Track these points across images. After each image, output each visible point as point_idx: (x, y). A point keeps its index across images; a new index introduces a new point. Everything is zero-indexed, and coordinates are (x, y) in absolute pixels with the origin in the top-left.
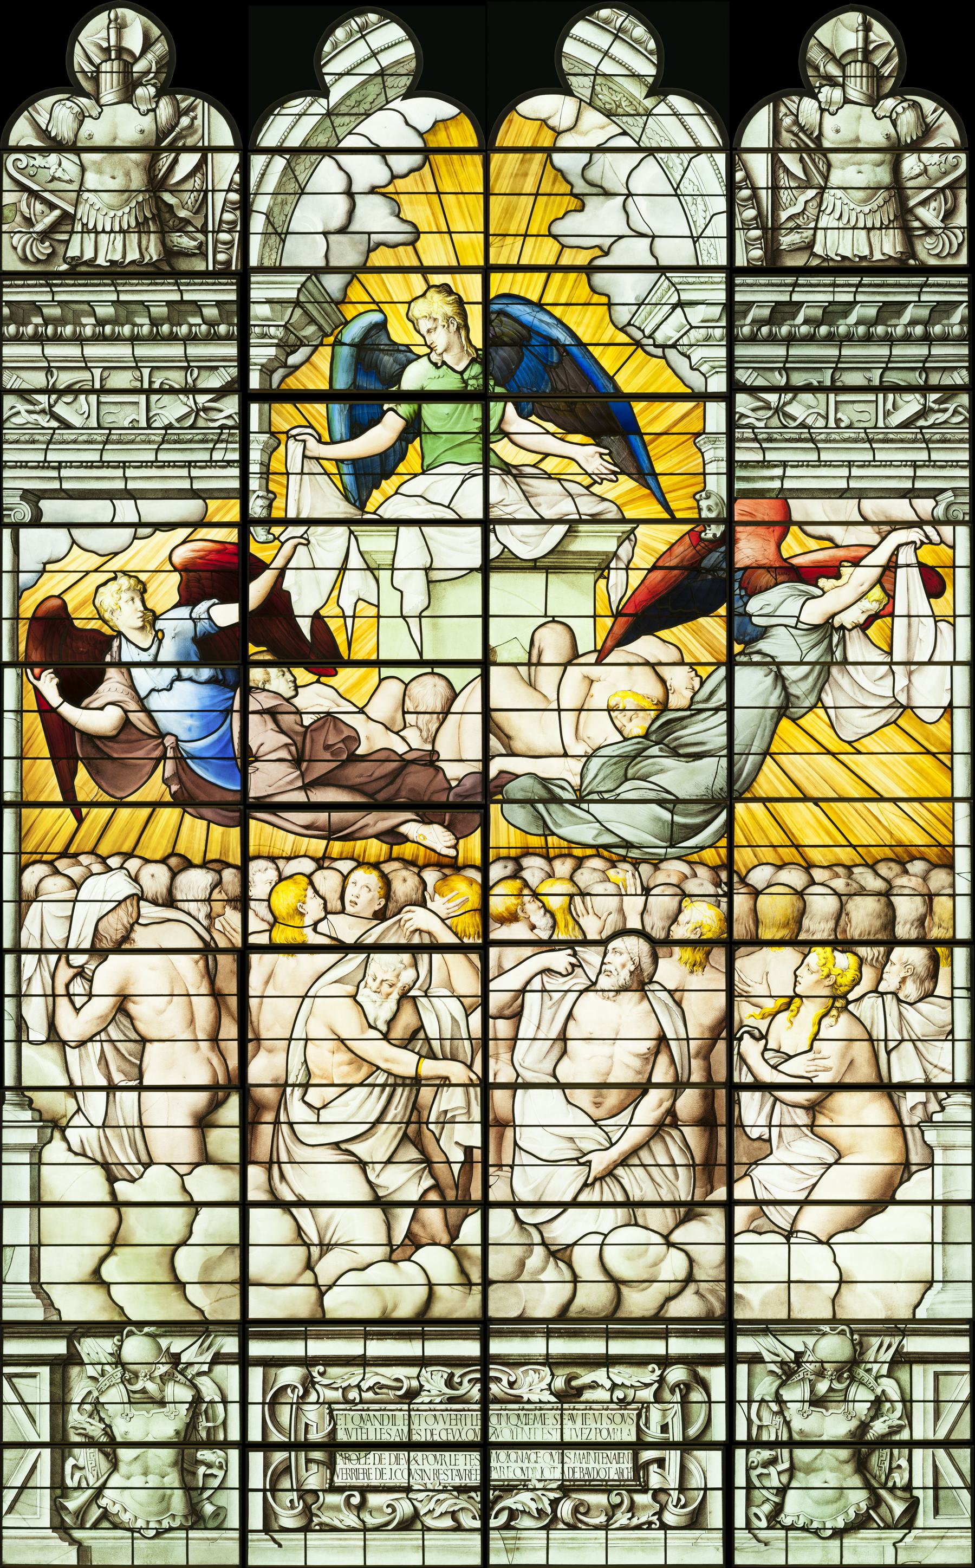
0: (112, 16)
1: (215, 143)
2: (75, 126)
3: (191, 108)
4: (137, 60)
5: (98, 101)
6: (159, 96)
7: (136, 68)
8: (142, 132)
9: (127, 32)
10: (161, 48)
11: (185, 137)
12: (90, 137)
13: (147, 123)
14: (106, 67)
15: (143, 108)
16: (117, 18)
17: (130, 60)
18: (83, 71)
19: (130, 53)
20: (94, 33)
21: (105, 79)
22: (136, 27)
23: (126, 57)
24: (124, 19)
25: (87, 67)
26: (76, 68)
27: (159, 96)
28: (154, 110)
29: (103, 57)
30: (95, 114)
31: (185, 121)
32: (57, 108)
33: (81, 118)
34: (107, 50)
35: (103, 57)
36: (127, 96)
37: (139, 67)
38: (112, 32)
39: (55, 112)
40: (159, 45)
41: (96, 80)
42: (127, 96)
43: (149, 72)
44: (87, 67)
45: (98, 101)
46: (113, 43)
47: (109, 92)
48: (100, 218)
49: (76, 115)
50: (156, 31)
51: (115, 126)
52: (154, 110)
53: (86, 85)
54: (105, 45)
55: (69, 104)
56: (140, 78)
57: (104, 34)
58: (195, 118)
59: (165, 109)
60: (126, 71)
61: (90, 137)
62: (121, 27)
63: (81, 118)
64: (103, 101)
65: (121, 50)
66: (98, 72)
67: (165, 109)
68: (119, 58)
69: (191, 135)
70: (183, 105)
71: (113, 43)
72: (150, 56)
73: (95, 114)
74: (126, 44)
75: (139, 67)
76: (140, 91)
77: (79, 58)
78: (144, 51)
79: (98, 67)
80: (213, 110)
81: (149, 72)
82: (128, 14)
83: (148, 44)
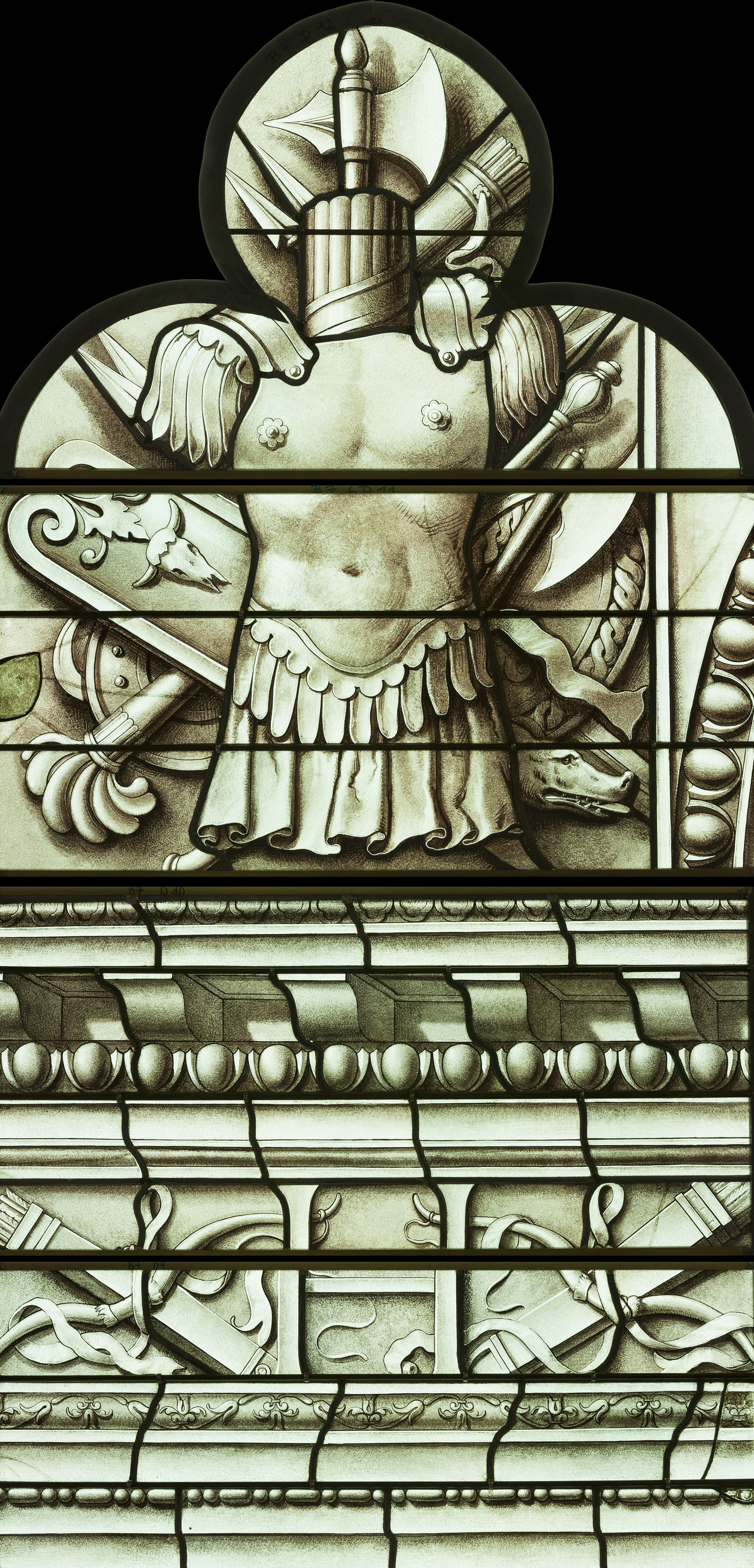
0: (349, 52)
1: (678, 461)
2: (231, 405)
3: (602, 348)
4: (426, 192)
5: (301, 325)
6: (498, 306)
7: (425, 220)
8: (444, 423)
9: (394, 103)
10: (504, 154)
11: (582, 441)
12: (278, 440)
13: (461, 394)
14: (329, 214)
15: (448, 347)
16: (362, 58)
17: (406, 193)
18: (254, 230)
19: (407, 169)
20: (290, 107)
21: (325, 254)
22: (424, 87)
23: (391, 183)
24: (386, 59)
25: (269, 217)
26: (233, 219)
27: (498, 306)
28: (482, 354)
29: (320, 184)
30: (292, 365)
31: (582, 390)
32: (173, 349)
33: (248, 377)
34: (332, 162)
35: (320, 184)
36: (396, 307)
37: (433, 216)
38: (349, 103)
39: (165, 361)
40: (498, 145)
41: (294, 256)
42: (396, 307)
43: (466, 231)
44: (269, 217)
45: (301, 325)
46: (350, 136)
47: (336, 304)
48: (310, 702)
49: (232, 371)
50: (488, 101)
51: (356, 405)
52: (482, 354)
53: (265, 274)
54: (325, 144)
55: (209, 334)
56: (438, 251)
57: (322, 109)
58: (615, 379)
59: (518, 350)
60: (393, 228)
61: (278, 440)
62: (376, 87)
63: (248, 377)
64: (318, 325)
65: (376, 161)
66: (303, 231)
67: (518, 350)
68: (369, 185)
69: (603, 433)
70: (577, 338)
71: (350, 138)
72: (468, 180)
73: (292, 365)
74: (393, 140)
75: (433, 216)
76: (438, 294)
77: (240, 190)
78: (451, 164)
79: (301, 215)
80: (671, 352)
81: (466, 231)
82: (401, 46)
83: (462, 141)
